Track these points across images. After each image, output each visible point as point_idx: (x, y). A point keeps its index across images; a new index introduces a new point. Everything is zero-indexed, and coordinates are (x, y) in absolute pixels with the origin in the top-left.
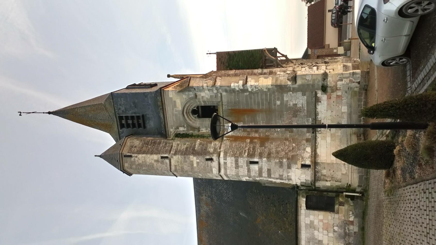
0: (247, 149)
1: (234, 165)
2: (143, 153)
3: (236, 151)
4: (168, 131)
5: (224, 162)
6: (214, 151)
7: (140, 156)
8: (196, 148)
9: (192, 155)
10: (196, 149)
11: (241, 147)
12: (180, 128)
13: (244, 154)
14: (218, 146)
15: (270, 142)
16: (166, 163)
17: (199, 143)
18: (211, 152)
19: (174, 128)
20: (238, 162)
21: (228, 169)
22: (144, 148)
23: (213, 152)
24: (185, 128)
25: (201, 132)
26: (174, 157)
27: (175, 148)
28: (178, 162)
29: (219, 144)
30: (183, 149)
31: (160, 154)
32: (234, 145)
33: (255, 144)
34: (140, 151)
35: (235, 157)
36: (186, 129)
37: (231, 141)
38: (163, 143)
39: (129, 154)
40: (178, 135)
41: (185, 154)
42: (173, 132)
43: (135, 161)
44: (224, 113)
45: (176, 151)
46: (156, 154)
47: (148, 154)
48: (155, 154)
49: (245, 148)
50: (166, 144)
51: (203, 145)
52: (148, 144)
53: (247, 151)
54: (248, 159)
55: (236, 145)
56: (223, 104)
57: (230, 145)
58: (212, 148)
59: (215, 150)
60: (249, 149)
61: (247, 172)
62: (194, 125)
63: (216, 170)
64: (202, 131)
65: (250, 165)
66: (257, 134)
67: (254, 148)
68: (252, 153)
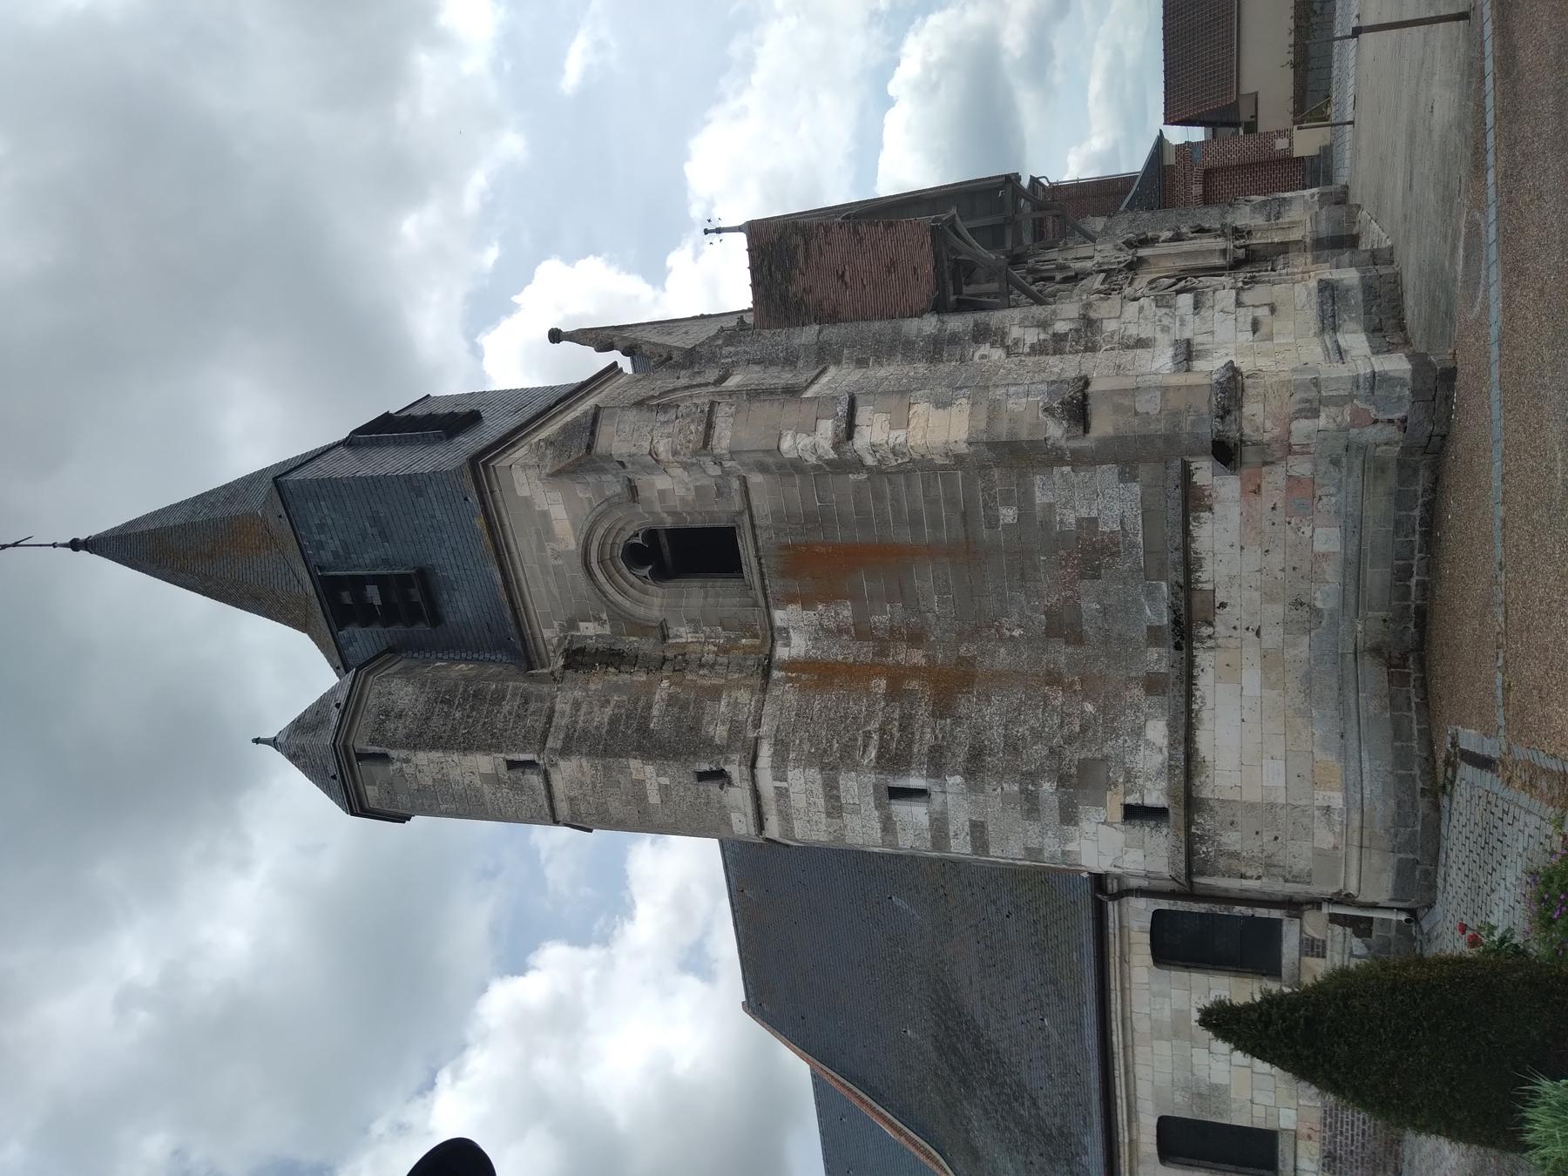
0: (874, 725)
1: (821, 802)
2: (433, 748)
3: (827, 735)
4: (534, 639)
5: (776, 788)
6: (729, 737)
7: (422, 757)
8: (655, 720)
9: (636, 758)
10: (652, 725)
11: (847, 718)
12: (582, 625)
13: (864, 752)
14: (746, 709)
15: (979, 694)
16: (532, 789)
17: (665, 696)
18: (719, 742)
19: (556, 624)
20: (837, 788)
21: (794, 816)
22: (436, 722)
23: (725, 742)
24: (602, 624)
25: (674, 641)
26: (562, 763)
27: (564, 722)
28: (581, 785)
29: (751, 701)
30: (597, 728)
31: (501, 752)
32: (817, 706)
33: (912, 704)
34: (420, 735)
35: (822, 769)
36: (607, 630)
37: (803, 688)
38: (514, 695)
39: (377, 749)
40: (579, 658)
41: (606, 753)
42: (555, 641)
43: (403, 776)
44: (763, 561)
45: (567, 736)
46: (485, 750)
47: (453, 748)
48: (479, 749)
49: (867, 723)
50: (526, 702)
51: (684, 707)
52: (449, 703)
53: (875, 737)
54: (881, 776)
55: (826, 707)
56: (757, 522)
57: (801, 706)
58: (723, 723)
59: (735, 730)
60: (882, 730)
61: (879, 830)
62: (641, 611)
63: (743, 819)
64: (677, 636)
65: (892, 801)
66: (920, 652)
67: (906, 724)
68: (897, 748)
